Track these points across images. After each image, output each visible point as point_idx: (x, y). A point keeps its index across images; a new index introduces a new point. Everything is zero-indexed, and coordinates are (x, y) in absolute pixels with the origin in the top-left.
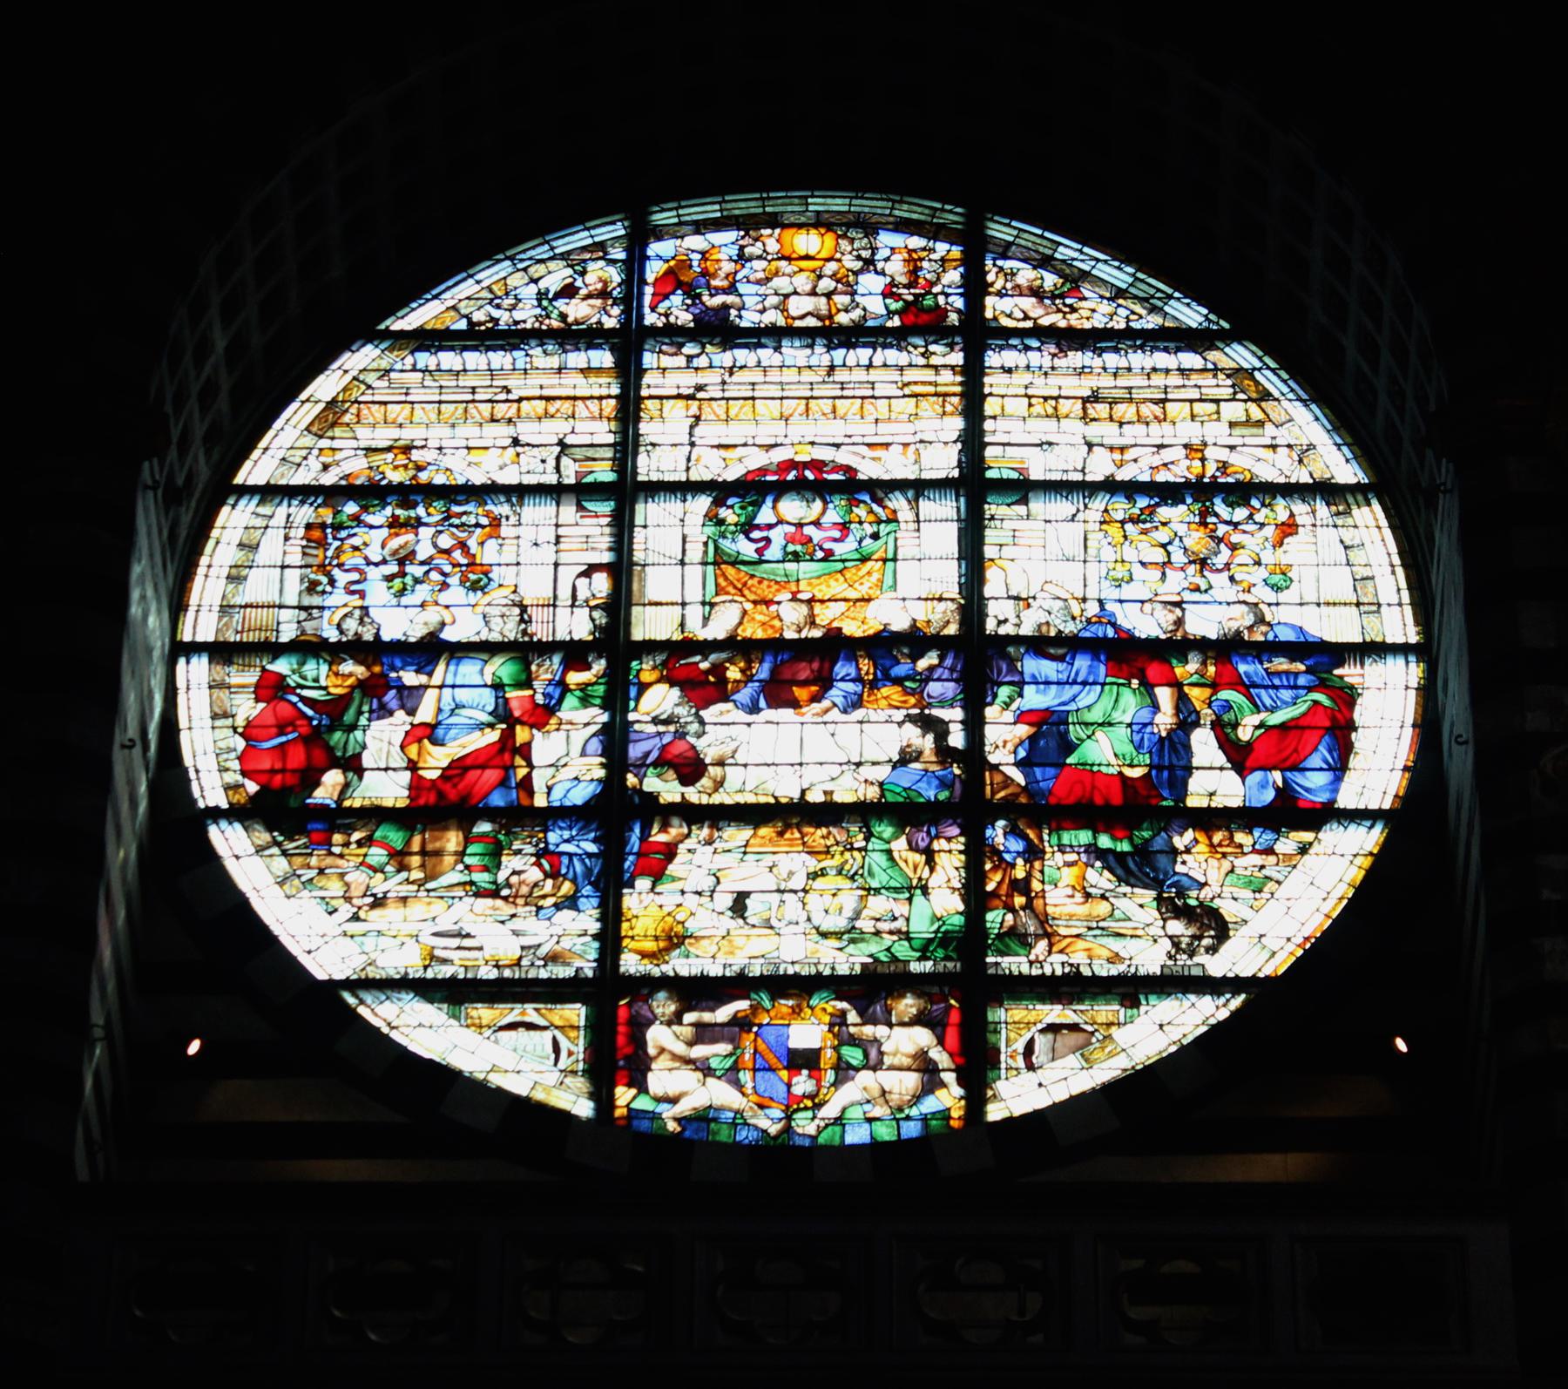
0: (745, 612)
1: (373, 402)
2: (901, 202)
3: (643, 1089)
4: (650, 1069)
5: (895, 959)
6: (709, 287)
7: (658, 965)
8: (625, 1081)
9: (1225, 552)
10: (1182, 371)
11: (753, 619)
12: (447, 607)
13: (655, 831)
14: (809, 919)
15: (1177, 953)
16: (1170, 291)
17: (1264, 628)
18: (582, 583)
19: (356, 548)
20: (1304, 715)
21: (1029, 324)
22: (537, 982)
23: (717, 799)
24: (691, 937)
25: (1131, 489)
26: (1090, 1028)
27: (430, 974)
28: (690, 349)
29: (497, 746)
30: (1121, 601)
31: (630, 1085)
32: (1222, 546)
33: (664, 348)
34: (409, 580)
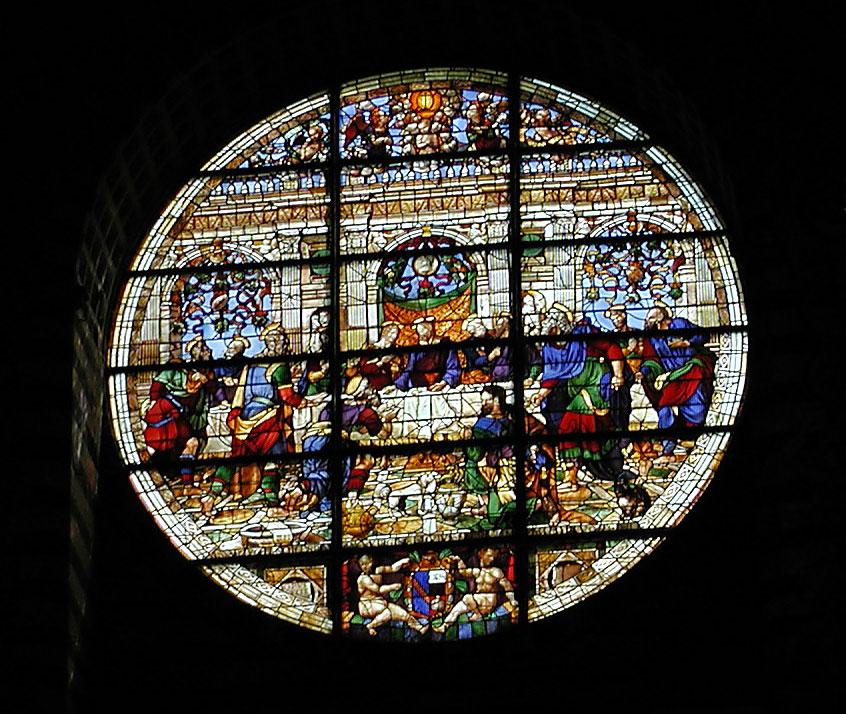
0: (399, 330)
1: (202, 216)
3: (357, 612)
4: (359, 600)
5: (481, 529)
6: (374, 133)
7: (361, 541)
10: (626, 169)
12: (246, 338)
13: (358, 461)
14: (438, 510)
16: (618, 118)
17: (668, 322)
20: (689, 372)
26: (581, 562)
30: (594, 311)
32: (646, 274)
33: (352, 172)
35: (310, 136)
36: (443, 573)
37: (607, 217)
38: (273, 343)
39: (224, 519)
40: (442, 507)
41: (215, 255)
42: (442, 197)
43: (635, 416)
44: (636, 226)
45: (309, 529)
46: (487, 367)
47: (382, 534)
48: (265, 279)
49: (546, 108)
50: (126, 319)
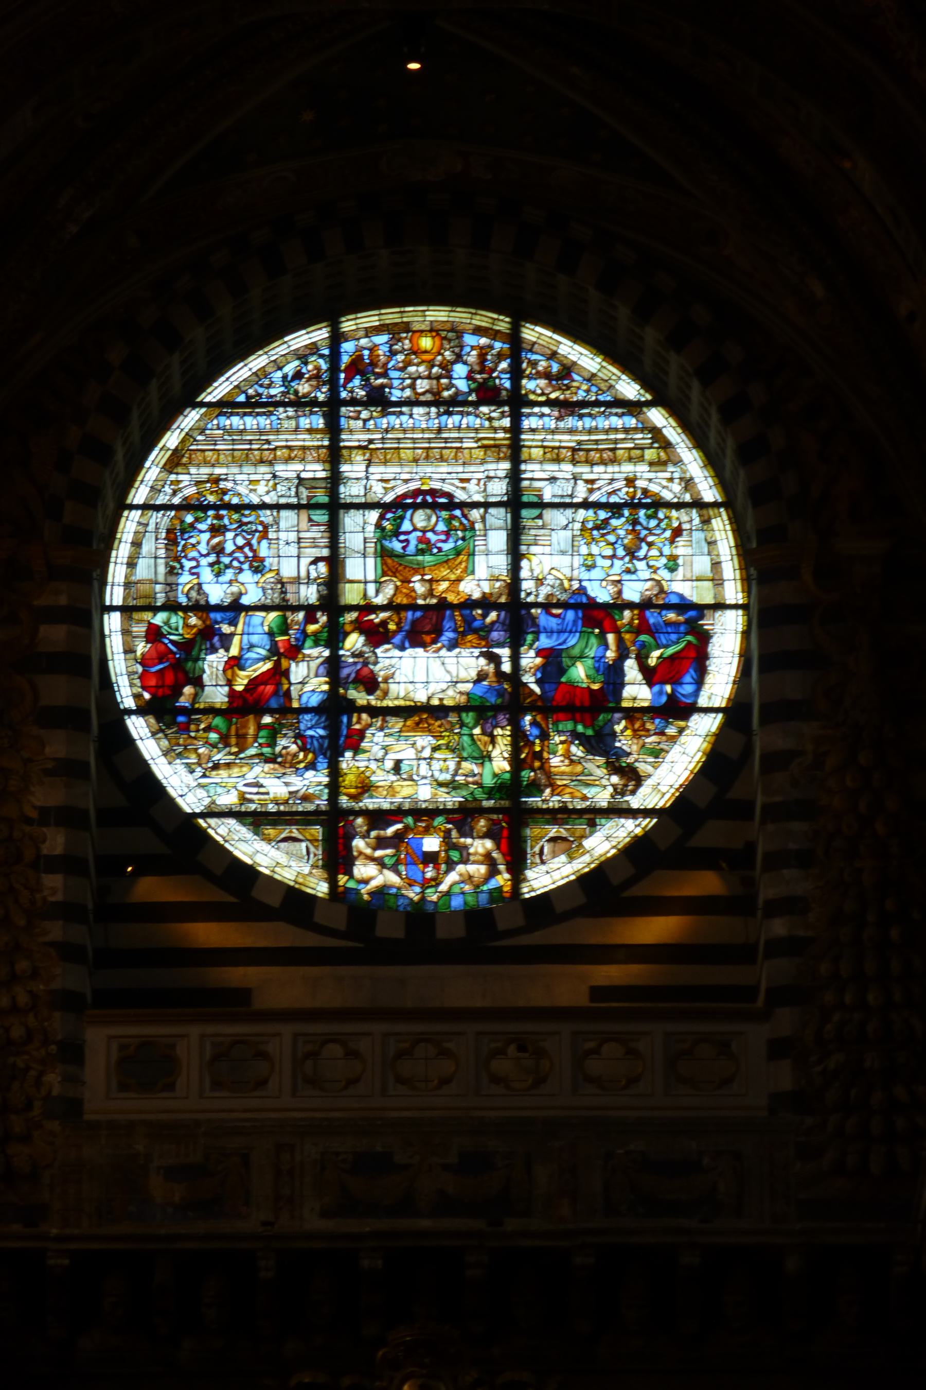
0: (397, 588)
3: (351, 876)
5: (475, 799)
6: (374, 374)
8: (343, 871)
9: (644, 547)
10: (626, 430)
12: (243, 584)
16: (619, 373)
17: (663, 596)
18: (313, 567)
19: (194, 546)
21: (543, 399)
23: (386, 703)
24: (372, 786)
25: (597, 505)
27: (243, 809)
28: (365, 414)
31: (345, 874)
34: (222, 566)
38: (269, 591)
41: (212, 493)
43: (627, 692)
44: (635, 492)
46: (482, 634)
47: (377, 798)
48: (262, 523)
50: (120, 555)
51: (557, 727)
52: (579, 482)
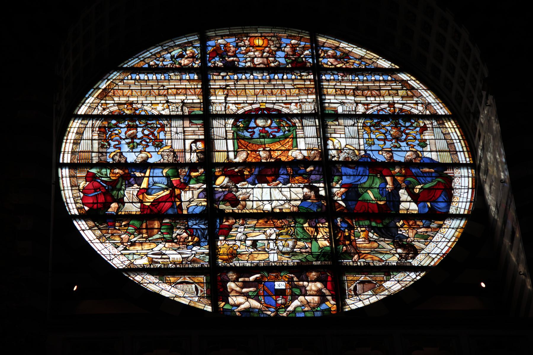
0: (248, 154)
1: (119, 89)
2: (288, 30)
3: (227, 302)
5: (308, 261)
7: (229, 263)
8: (221, 299)
11: (251, 156)
12: (149, 152)
13: (224, 221)
14: (278, 248)
15: (401, 259)
16: (378, 57)
17: (419, 159)
19: (116, 134)
20: (435, 185)
22: (189, 268)
23: (244, 211)
26: (375, 282)
27: (152, 266)
29: (169, 195)
30: (372, 150)
32: (403, 134)
34: (135, 144)
35: (187, 54)
36: (284, 283)
37: (376, 105)
38: (166, 156)
39: (136, 247)
40: (281, 248)
41: (128, 110)
42: (272, 89)
43: (403, 206)
44: (394, 109)
45: (193, 255)
47: (242, 260)
49: (333, 50)
51: (359, 223)
52: (359, 105)
